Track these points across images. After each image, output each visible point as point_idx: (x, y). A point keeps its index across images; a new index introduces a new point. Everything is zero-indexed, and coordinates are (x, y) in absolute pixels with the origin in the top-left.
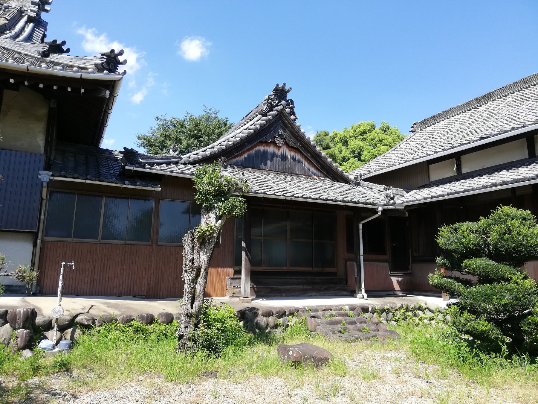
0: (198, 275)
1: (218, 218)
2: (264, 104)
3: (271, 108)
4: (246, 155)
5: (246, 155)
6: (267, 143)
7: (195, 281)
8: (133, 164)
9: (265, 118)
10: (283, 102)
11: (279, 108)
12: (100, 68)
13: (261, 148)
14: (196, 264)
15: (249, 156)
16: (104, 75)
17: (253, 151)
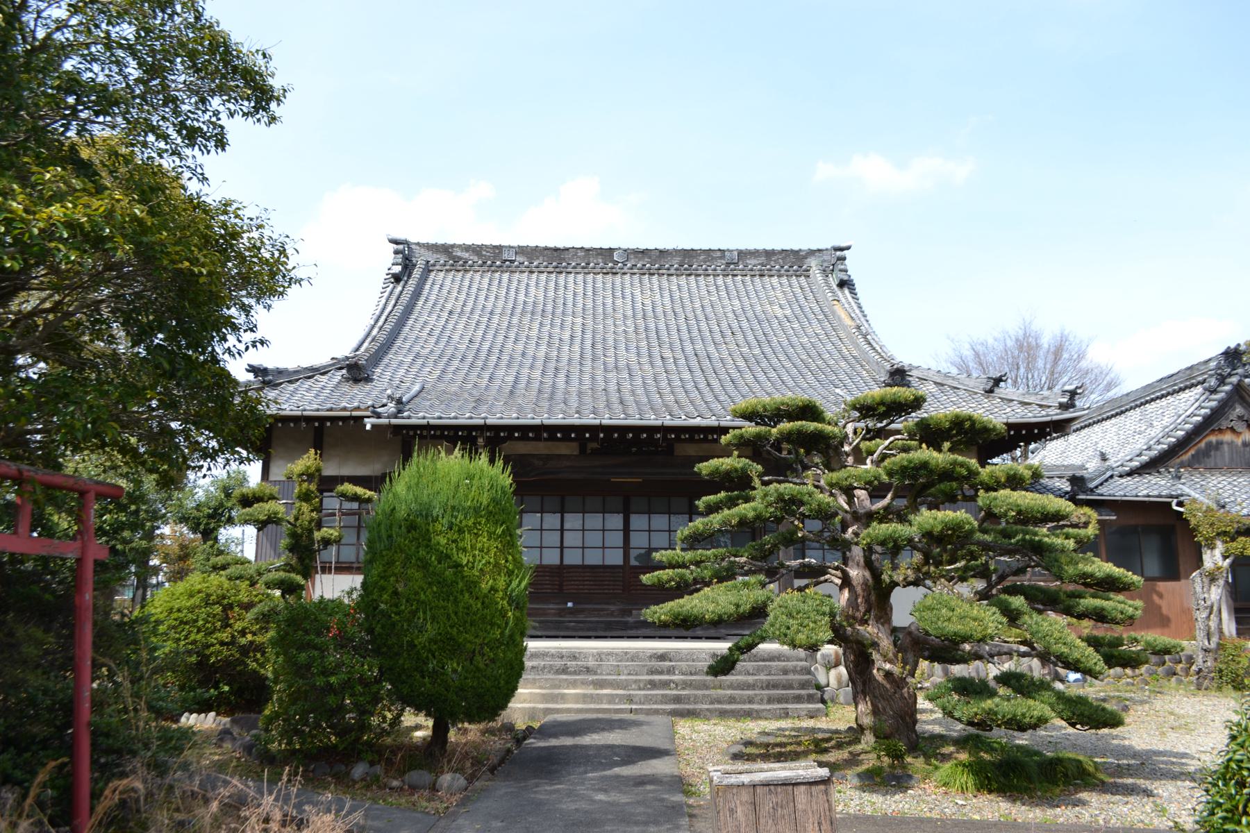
0: (1211, 613)
1: (1225, 558)
2: (1211, 376)
3: (1222, 380)
4: (1192, 452)
5: (1192, 452)
6: (1220, 431)
7: (1208, 618)
8: (1084, 492)
9: (1213, 397)
10: (1240, 371)
11: (1234, 379)
12: (1064, 407)
13: (1213, 438)
14: (1209, 603)
15: (1198, 452)
17: (1203, 444)
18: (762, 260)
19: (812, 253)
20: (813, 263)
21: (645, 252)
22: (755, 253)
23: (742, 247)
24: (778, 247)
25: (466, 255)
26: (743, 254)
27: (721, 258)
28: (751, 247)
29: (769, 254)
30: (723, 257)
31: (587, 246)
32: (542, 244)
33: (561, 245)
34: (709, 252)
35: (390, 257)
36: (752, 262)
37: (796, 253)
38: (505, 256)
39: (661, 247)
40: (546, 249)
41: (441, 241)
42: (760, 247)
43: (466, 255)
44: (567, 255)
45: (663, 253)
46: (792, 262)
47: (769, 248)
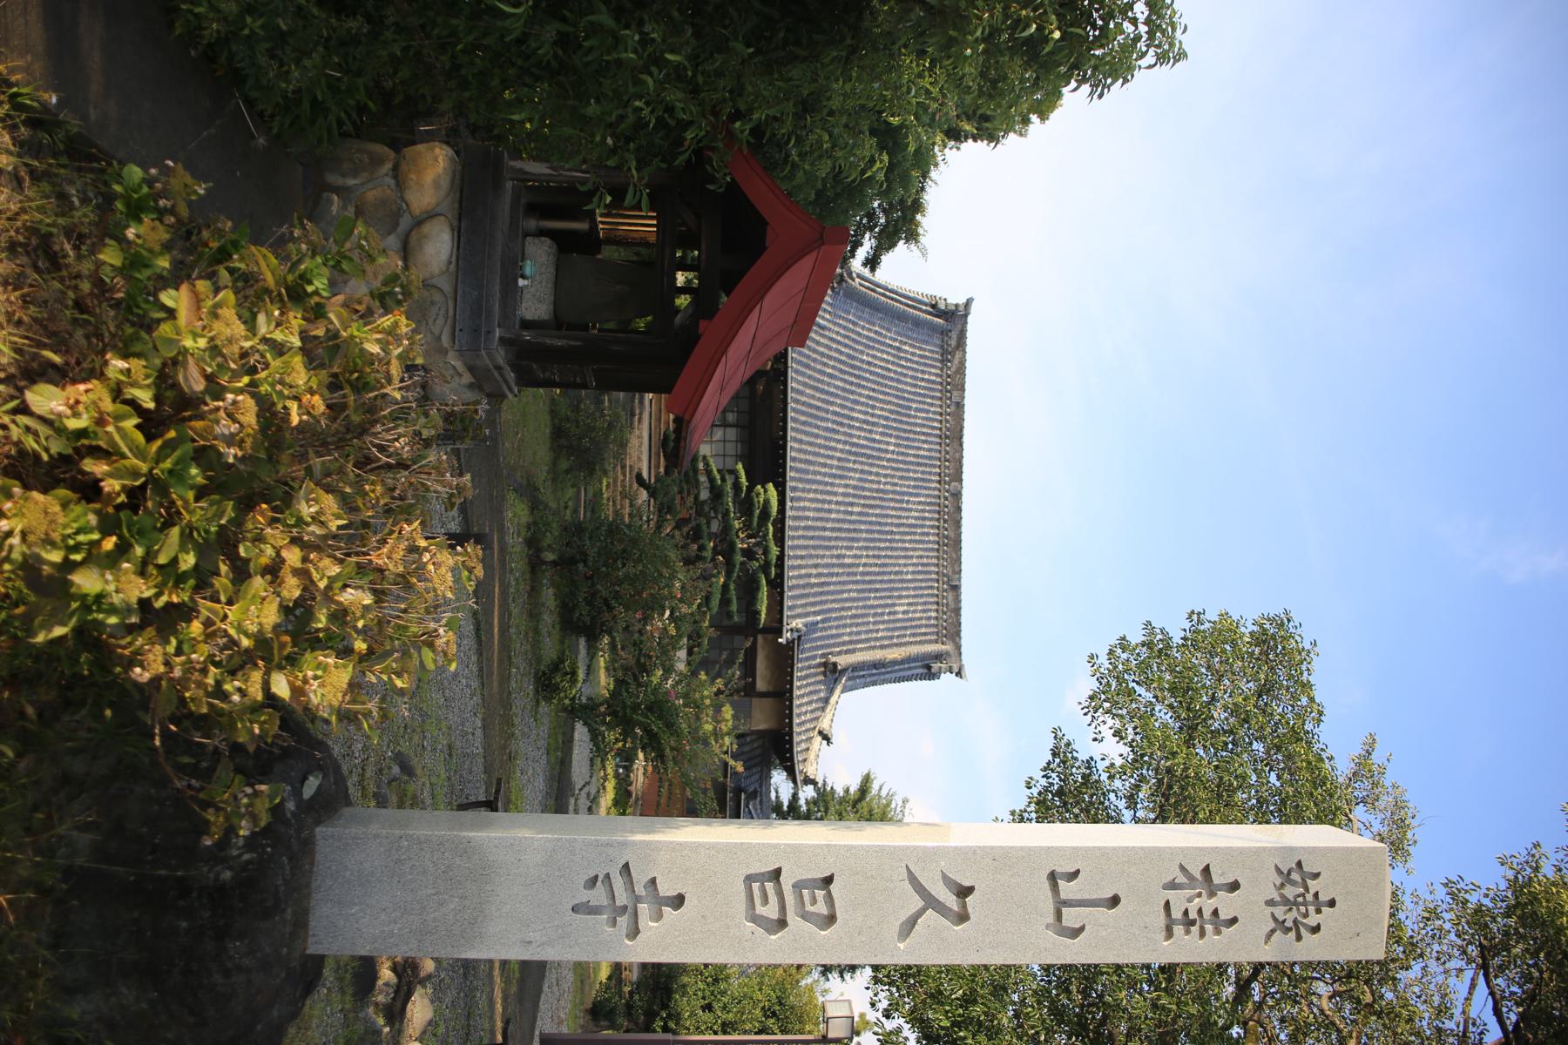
16: (799, 778)
18: (952, 605)
19: (958, 647)
20: (948, 647)
21: (959, 509)
22: (958, 600)
23: (963, 589)
24: (963, 620)
25: (956, 361)
26: (956, 589)
27: (954, 572)
28: (963, 597)
29: (957, 611)
30: (954, 572)
31: (965, 461)
32: (966, 424)
33: (965, 439)
34: (958, 561)
35: (952, 300)
36: (950, 596)
37: (958, 633)
38: (955, 393)
39: (964, 522)
40: (962, 428)
41: (968, 341)
42: (963, 604)
43: (956, 361)
44: (956, 444)
45: (958, 524)
46: (951, 631)
47: (963, 612)
